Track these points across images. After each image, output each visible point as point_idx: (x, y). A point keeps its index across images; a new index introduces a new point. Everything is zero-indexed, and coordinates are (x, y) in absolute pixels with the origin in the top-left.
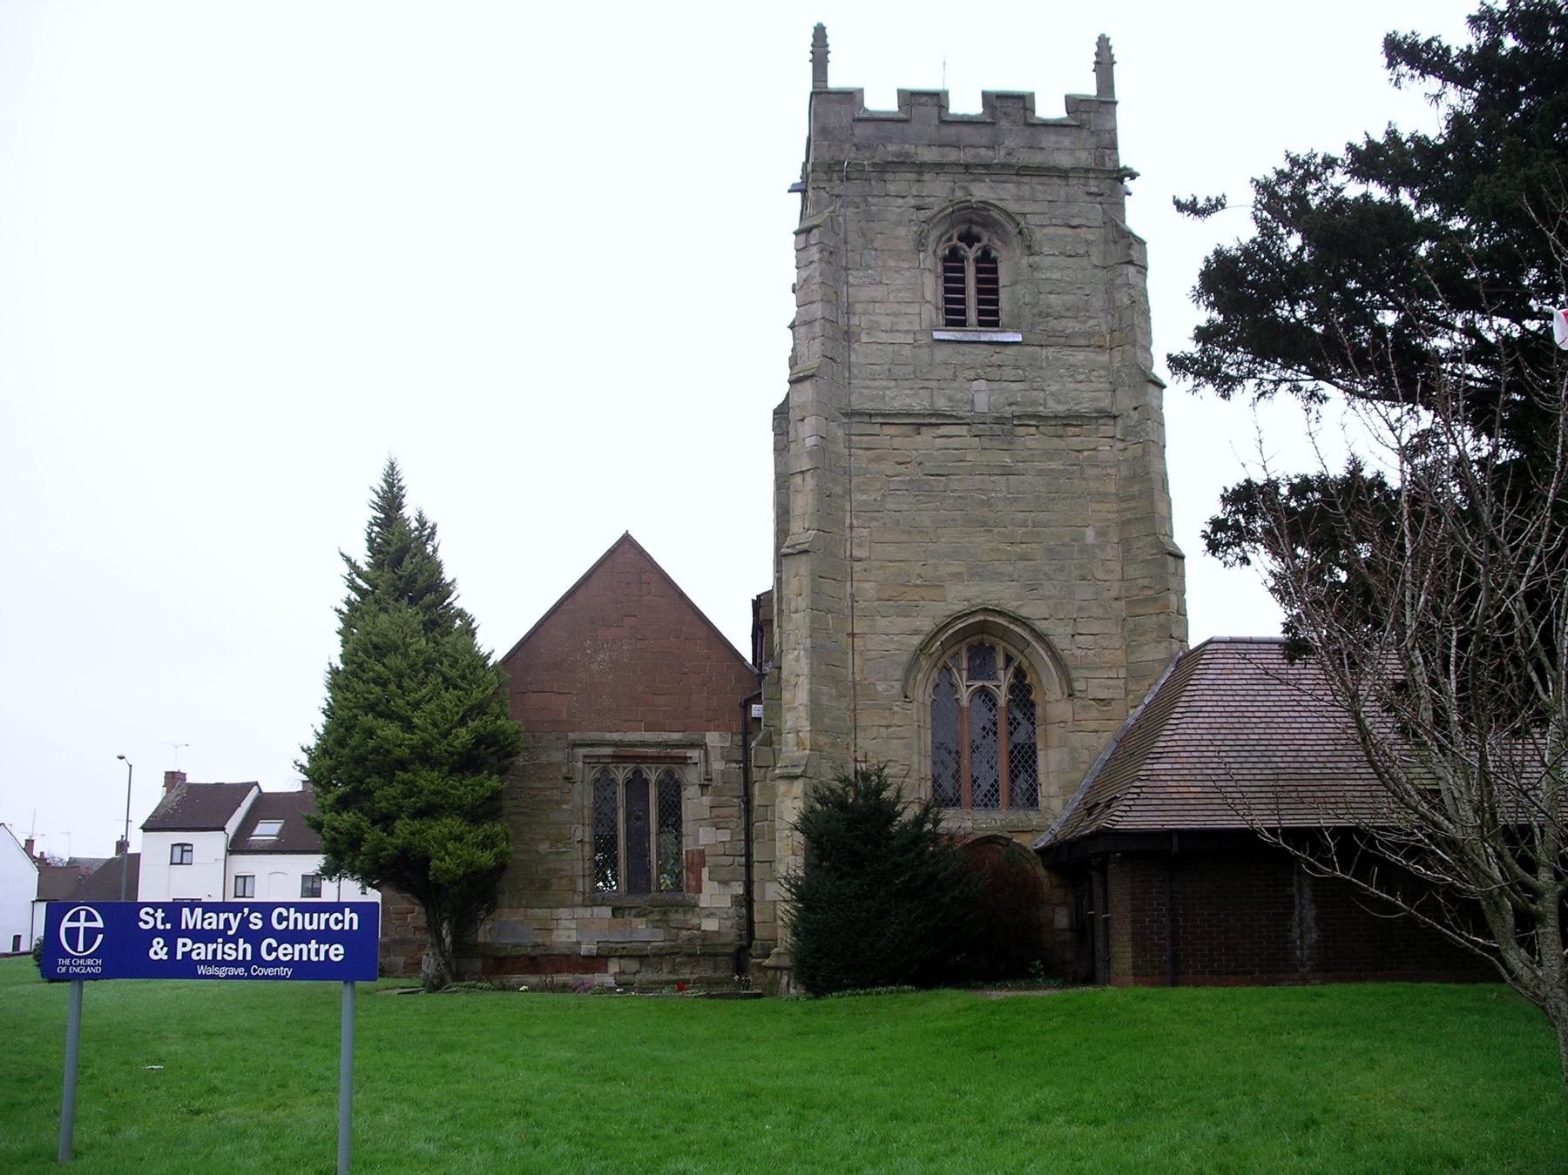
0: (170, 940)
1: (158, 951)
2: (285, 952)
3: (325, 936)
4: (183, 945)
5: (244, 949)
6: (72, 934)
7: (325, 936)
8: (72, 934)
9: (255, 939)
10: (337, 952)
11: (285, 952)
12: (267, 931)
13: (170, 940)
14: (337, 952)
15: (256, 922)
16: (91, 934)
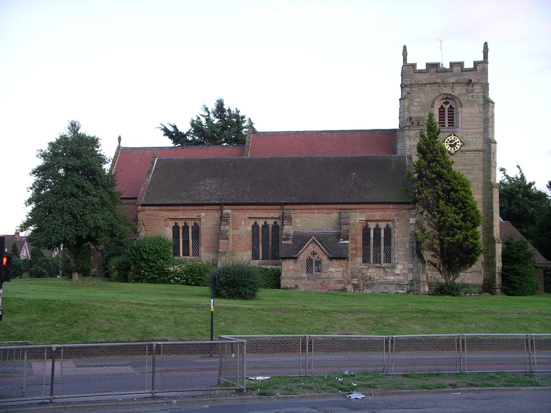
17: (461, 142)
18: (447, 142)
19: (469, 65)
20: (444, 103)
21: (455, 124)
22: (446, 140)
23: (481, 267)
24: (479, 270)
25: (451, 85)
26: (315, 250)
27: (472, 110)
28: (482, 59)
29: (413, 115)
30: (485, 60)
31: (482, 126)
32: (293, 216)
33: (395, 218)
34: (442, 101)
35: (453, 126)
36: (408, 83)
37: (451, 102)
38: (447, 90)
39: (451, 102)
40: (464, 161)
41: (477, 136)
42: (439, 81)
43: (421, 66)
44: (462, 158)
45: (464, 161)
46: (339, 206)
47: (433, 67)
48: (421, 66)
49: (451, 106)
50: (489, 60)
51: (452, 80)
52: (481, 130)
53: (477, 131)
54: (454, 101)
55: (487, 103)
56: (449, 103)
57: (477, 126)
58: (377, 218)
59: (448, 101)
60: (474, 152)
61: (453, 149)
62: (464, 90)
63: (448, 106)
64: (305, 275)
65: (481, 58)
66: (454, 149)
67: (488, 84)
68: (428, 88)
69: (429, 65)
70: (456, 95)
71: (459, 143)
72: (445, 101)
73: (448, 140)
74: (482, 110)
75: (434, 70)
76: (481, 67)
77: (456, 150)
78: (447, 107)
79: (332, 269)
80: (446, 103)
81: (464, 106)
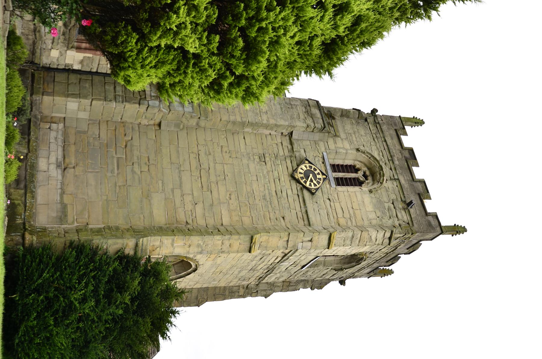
17: (317, 190)
18: (311, 167)
19: (430, 206)
20: (365, 173)
22: (313, 167)
23: (76, 224)
24: (70, 219)
25: (396, 177)
27: (370, 208)
28: (443, 224)
30: (443, 230)
34: (365, 169)
40: (284, 194)
41: (331, 217)
43: (407, 142)
44: (289, 192)
45: (284, 194)
47: (410, 157)
53: (340, 215)
56: (367, 179)
57: (347, 215)
59: (370, 178)
60: (304, 210)
61: (302, 175)
62: (393, 197)
63: (362, 179)
66: (302, 178)
68: (380, 144)
69: (411, 151)
71: (313, 187)
72: (368, 173)
73: (315, 170)
76: (434, 227)
77: (302, 181)
78: (360, 175)
81: (372, 195)
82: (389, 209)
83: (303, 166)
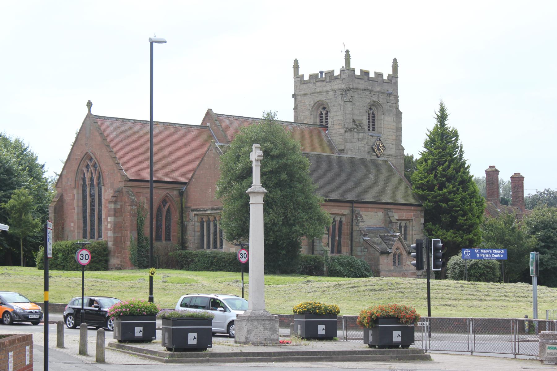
0: (480, 254)
1: (478, 255)
2: (495, 256)
3: (500, 254)
4: (481, 255)
5: (489, 255)
6: (466, 253)
7: (500, 254)
8: (466, 253)
9: (491, 254)
10: (502, 256)
11: (495, 256)
12: (492, 253)
13: (480, 254)
14: (502, 256)
15: (491, 252)
16: (468, 253)
19: (385, 77)
21: (376, 129)
26: (398, 245)
29: (355, 118)
31: (395, 134)
32: (361, 213)
33: (413, 218)
35: (374, 130)
36: (351, 87)
37: (374, 108)
38: (375, 99)
39: (374, 108)
42: (370, 88)
46: (384, 206)
48: (358, 73)
49: (373, 112)
50: (399, 75)
51: (378, 89)
52: (394, 137)
54: (377, 108)
55: (399, 114)
58: (404, 218)
59: (372, 107)
63: (371, 112)
64: (393, 268)
65: (391, 73)
67: (398, 97)
70: (381, 103)
74: (395, 119)
75: (366, 77)
79: (409, 263)
80: (370, 109)
82: (390, 106)
83: (376, 150)
